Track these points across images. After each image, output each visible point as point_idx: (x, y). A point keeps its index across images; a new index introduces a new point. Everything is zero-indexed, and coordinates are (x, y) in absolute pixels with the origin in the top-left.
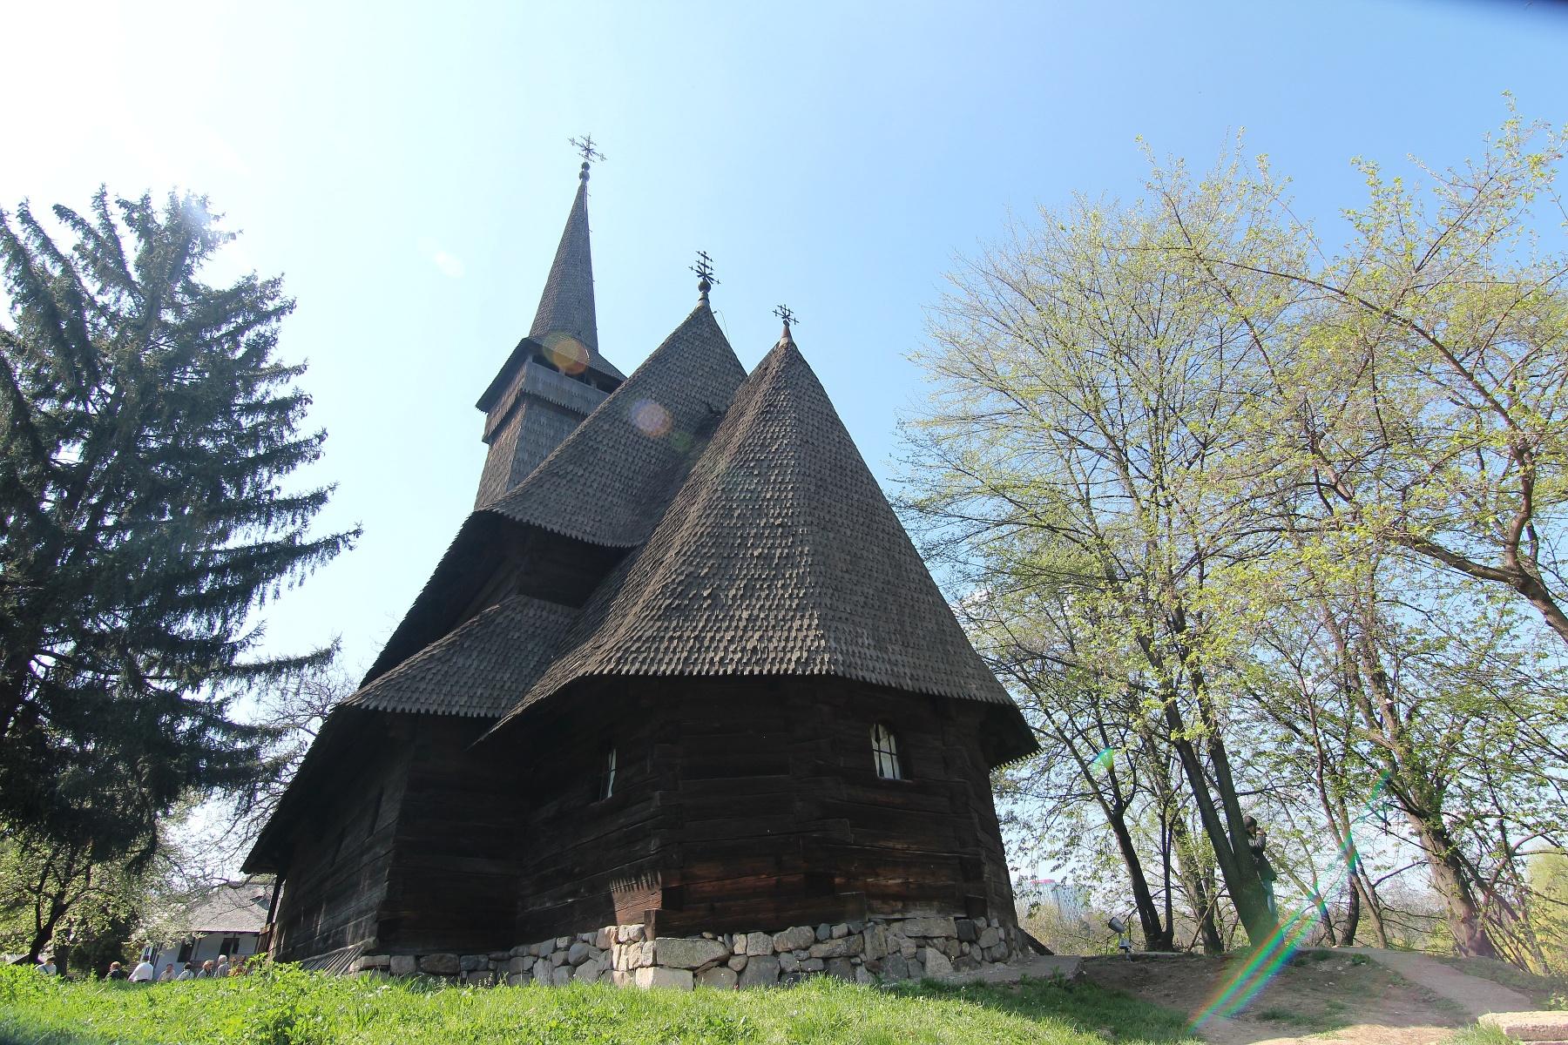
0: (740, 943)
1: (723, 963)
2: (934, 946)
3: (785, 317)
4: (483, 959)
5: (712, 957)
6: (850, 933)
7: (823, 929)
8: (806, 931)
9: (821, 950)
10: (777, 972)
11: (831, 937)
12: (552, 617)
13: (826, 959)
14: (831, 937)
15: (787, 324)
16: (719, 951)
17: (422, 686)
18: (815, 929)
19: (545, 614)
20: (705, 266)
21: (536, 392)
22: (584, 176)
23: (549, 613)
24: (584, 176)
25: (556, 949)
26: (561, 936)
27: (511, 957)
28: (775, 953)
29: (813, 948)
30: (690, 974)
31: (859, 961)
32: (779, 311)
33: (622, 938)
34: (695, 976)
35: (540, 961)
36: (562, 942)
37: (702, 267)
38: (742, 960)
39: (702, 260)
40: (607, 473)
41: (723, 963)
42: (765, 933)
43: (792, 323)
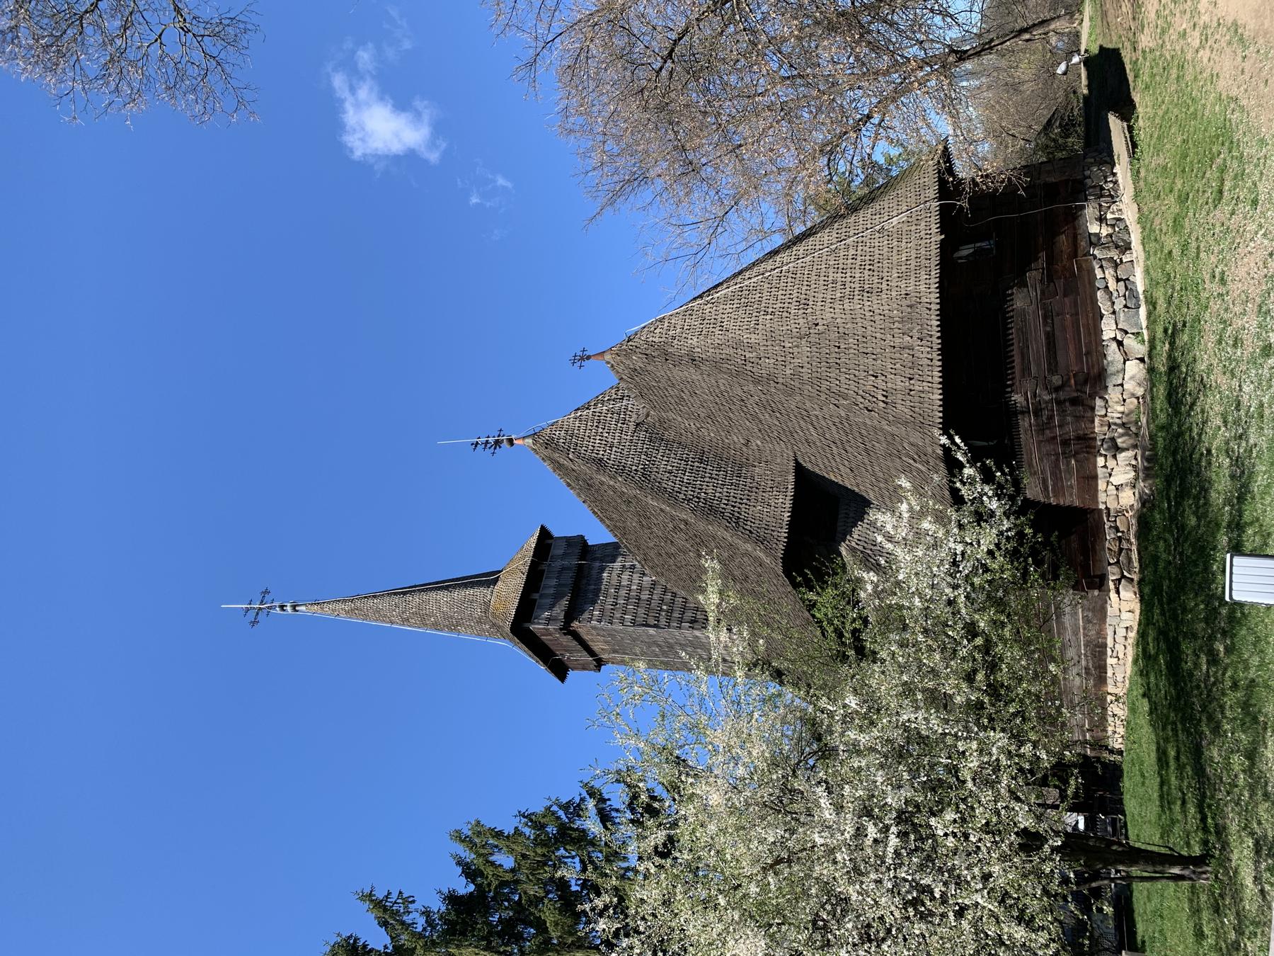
0: (1108, 330)
1: (1120, 344)
2: (1106, 213)
3: (582, 359)
5: (1117, 350)
6: (1101, 267)
8: (1099, 294)
9: (1112, 285)
10: (1126, 310)
11: (1104, 278)
12: (852, 515)
13: (1118, 280)
14: (1104, 278)
15: (589, 358)
16: (1114, 345)
18: (1099, 289)
23: (848, 518)
25: (1105, 466)
26: (1096, 461)
27: (1107, 508)
28: (1114, 312)
29: (1111, 289)
30: (1127, 362)
31: (1118, 260)
32: (579, 364)
33: (1103, 412)
34: (1128, 360)
35: (1112, 479)
37: (489, 445)
38: (1117, 332)
40: (725, 490)
41: (1120, 344)
42: (1102, 319)
43: (587, 353)
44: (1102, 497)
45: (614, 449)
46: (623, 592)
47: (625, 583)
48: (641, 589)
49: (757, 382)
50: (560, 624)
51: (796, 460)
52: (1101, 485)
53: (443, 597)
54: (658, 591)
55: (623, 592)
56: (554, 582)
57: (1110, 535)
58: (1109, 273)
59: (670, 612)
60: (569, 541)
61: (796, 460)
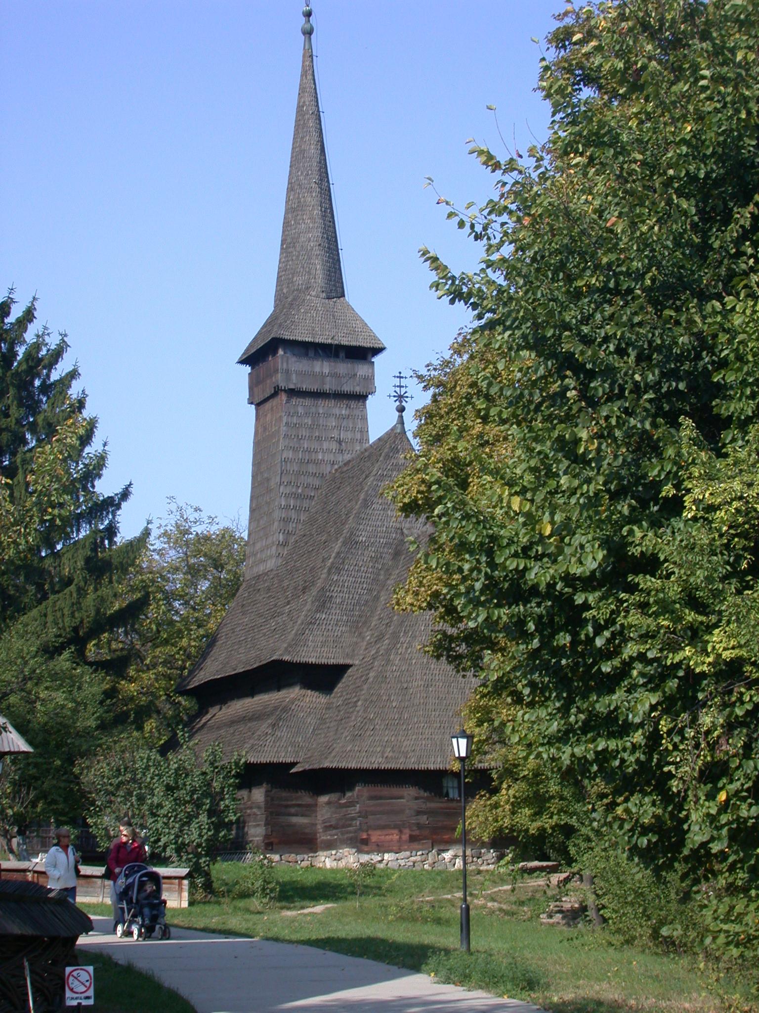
0: (387, 856)
4: (306, 857)
7: (414, 853)
8: (408, 853)
9: (412, 859)
13: (414, 863)
16: (380, 859)
17: (266, 748)
19: (314, 700)
20: (400, 387)
21: (292, 386)
22: (308, 33)
24: (308, 33)
36: (334, 852)
37: (398, 389)
39: (397, 381)
44: (320, 853)
45: (382, 512)
46: (314, 445)
47: (325, 445)
48: (317, 463)
49: (388, 651)
50: (282, 385)
51: (351, 666)
52: (325, 853)
53: (316, 234)
54: (317, 482)
55: (314, 445)
56: (326, 370)
57: (299, 857)
58: (418, 858)
59: (297, 496)
60: (369, 379)
61: (351, 666)
